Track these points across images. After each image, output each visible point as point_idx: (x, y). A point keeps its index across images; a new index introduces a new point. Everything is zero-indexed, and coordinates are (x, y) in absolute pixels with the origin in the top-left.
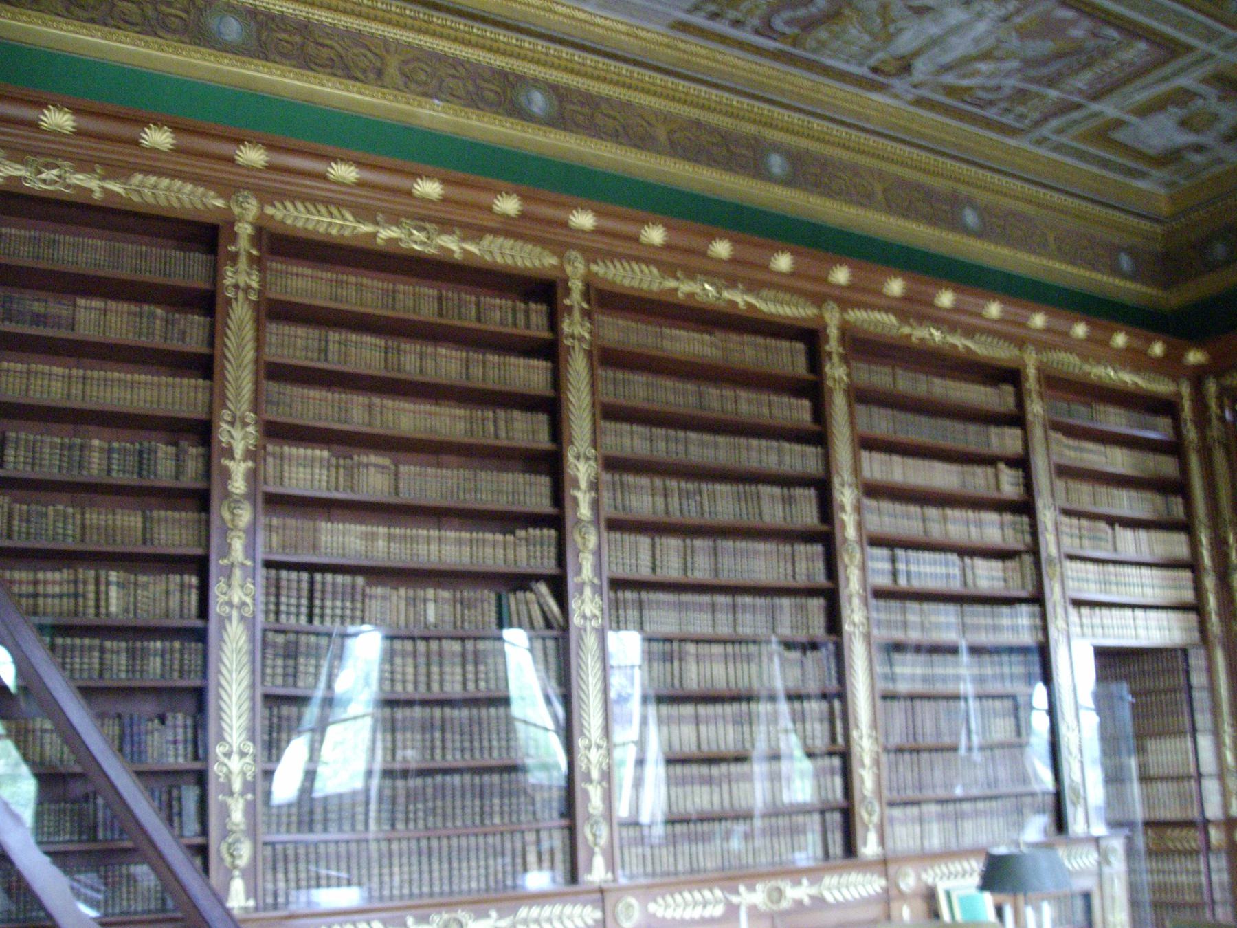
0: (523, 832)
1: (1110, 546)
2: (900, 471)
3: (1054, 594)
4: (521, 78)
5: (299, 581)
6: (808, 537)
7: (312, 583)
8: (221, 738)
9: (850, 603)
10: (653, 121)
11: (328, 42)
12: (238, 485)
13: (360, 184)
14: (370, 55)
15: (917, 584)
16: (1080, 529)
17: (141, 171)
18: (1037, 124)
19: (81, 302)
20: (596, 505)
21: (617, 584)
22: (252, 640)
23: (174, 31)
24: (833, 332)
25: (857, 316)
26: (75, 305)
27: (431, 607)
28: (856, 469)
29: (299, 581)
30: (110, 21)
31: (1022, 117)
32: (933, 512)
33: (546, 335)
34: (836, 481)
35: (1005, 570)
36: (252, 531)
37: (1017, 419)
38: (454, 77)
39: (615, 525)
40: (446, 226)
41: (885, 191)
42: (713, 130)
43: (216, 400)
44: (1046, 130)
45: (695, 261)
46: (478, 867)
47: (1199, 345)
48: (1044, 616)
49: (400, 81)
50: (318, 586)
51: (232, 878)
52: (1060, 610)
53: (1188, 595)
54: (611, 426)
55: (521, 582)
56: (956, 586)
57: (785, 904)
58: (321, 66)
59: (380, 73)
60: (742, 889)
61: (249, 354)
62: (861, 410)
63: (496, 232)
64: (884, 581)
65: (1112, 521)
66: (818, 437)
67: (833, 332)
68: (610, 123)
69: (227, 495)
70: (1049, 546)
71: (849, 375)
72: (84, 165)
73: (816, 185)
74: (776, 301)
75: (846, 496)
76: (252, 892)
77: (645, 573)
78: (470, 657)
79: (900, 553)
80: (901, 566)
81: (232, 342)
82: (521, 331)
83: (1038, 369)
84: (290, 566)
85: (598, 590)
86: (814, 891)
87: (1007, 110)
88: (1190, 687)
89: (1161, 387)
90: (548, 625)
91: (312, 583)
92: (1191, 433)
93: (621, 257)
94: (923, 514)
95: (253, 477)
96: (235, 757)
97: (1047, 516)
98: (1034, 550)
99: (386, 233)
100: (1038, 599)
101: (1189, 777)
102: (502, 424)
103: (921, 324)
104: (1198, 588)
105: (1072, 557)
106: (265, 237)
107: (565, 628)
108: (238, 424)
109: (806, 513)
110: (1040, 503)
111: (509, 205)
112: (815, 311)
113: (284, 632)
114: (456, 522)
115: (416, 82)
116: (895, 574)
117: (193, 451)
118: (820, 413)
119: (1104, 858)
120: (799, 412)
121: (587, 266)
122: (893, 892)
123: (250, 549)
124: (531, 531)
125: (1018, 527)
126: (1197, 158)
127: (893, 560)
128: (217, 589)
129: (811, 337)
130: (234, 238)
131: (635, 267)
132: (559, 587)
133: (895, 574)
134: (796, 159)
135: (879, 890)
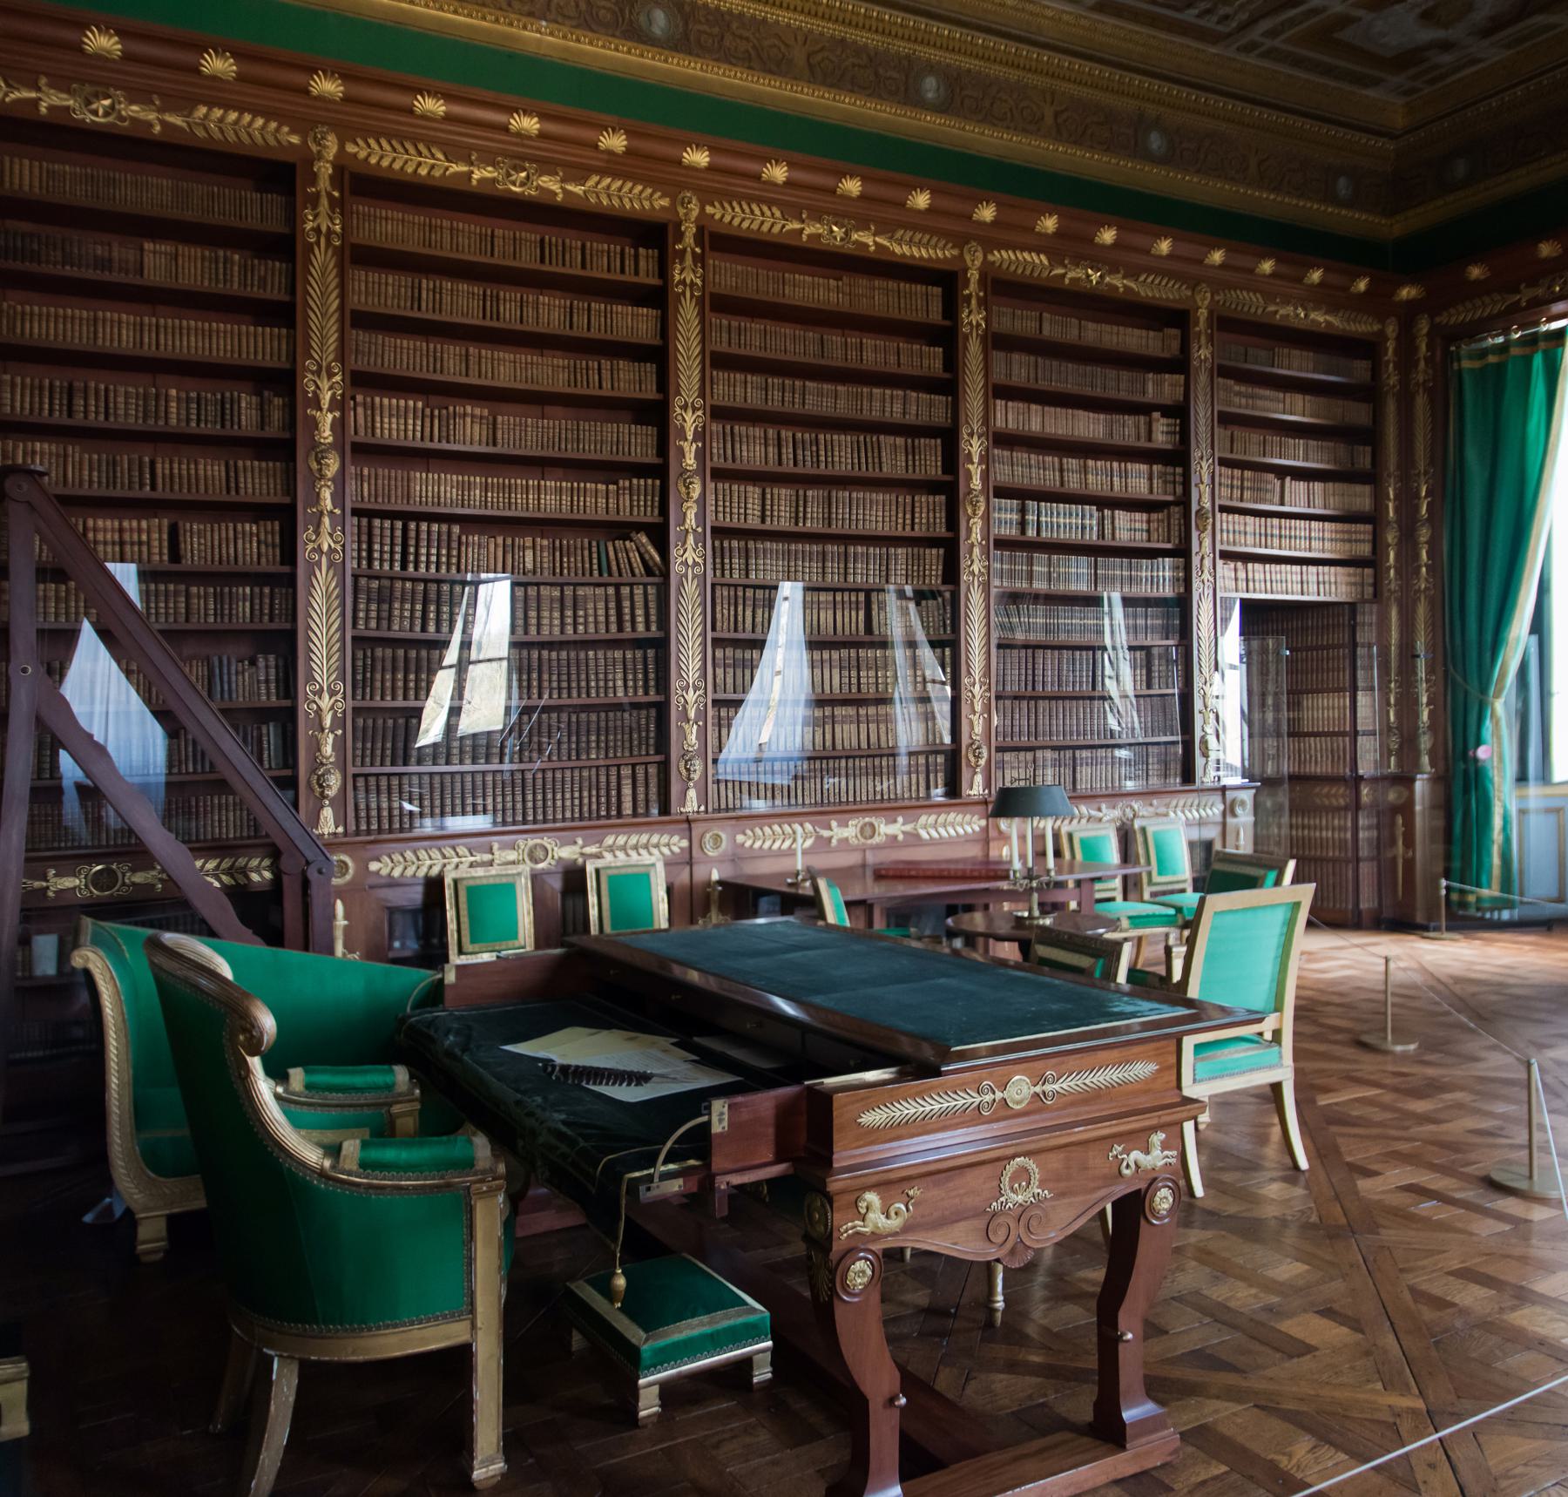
1: (1277, 499)
2: (1037, 420)
3: (1202, 546)
5: (392, 529)
6: (931, 487)
7: (405, 530)
8: (310, 678)
9: (971, 553)
12: (326, 434)
13: (448, 118)
16: (1242, 480)
17: (205, 104)
18: (1245, 27)
19: (148, 246)
20: (701, 455)
21: (719, 532)
22: (342, 584)
25: (1000, 256)
26: (142, 249)
27: (529, 554)
28: (986, 420)
29: (392, 529)
31: (1226, 17)
32: (1073, 463)
33: (654, 281)
34: (964, 432)
35: (1149, 522)
36: (340, 480)
37: (1180, 365)
39: (719, 475)
41: (1056, 115)
42: (859, 50)
43: (296, 349)
44: (1256, 33)
46: (573, 798)
47: (1412, 282)
48: (1188, 568)
50: (412, 534)
51: (322, 807)
52: (1208, 563)
53: (1365, 549)
54: (721, 375)
55: (621, 530)
56: (1092, 537)
57: (877, 840)
60: (834, 824)
62: (998, 356)
64: (1011, 532)
65: (1282, 472)
66: (948, 386)
69: (314, 445)
70: (1201, 496)
71: (986, 320)
74: (910, 242)
75: (974, 447)
76: (341, 819)
77: (753, 522)
78: (569, 603)
79: (1032, 505)
80: (1031, 517)
81: (315, 290)
82: (628, 277)
83: (1211, 313)
84: (384, 515)
85: (700, 539)
86: (908, 828)
87: (1208, 12)
88: (1354, 645)
89: (1363, 327)
90: (649, 571)
91: (405, 530)
92: (1392, 378)
94: (1061, 464)
95: (339, 426)
96: (326, 696)
97: (1203, 468)
98: (1184, 502)
99: (479, 174)
100: (1182, 552)
101: (1343, 734)
102: (606, 374)
103: (1077, 265)
104: (1377, 542)
105: (1223, 509)
106: (347, 176)
107: (666, 575)
108: (324, 373)
109: (930, 465)
110: (1195, 454)
112: (955, 252)
113: (377, 578)
116: (1023, 524)
117: (278, 401)
118: (952, 362)
119: (1230, 810)
120: (931, 360)
122: (992, 833)
123: (339, 498)
125: (1170, 478)
126: (1446, 58)
127: (1023, 511)
128: (305, 535)
129: (947, 280)
130: (313, 178)
131: (754, 207)
132: (660, 535)
133: (1023, 524)
134: (954, 81)
135: (977, 829)
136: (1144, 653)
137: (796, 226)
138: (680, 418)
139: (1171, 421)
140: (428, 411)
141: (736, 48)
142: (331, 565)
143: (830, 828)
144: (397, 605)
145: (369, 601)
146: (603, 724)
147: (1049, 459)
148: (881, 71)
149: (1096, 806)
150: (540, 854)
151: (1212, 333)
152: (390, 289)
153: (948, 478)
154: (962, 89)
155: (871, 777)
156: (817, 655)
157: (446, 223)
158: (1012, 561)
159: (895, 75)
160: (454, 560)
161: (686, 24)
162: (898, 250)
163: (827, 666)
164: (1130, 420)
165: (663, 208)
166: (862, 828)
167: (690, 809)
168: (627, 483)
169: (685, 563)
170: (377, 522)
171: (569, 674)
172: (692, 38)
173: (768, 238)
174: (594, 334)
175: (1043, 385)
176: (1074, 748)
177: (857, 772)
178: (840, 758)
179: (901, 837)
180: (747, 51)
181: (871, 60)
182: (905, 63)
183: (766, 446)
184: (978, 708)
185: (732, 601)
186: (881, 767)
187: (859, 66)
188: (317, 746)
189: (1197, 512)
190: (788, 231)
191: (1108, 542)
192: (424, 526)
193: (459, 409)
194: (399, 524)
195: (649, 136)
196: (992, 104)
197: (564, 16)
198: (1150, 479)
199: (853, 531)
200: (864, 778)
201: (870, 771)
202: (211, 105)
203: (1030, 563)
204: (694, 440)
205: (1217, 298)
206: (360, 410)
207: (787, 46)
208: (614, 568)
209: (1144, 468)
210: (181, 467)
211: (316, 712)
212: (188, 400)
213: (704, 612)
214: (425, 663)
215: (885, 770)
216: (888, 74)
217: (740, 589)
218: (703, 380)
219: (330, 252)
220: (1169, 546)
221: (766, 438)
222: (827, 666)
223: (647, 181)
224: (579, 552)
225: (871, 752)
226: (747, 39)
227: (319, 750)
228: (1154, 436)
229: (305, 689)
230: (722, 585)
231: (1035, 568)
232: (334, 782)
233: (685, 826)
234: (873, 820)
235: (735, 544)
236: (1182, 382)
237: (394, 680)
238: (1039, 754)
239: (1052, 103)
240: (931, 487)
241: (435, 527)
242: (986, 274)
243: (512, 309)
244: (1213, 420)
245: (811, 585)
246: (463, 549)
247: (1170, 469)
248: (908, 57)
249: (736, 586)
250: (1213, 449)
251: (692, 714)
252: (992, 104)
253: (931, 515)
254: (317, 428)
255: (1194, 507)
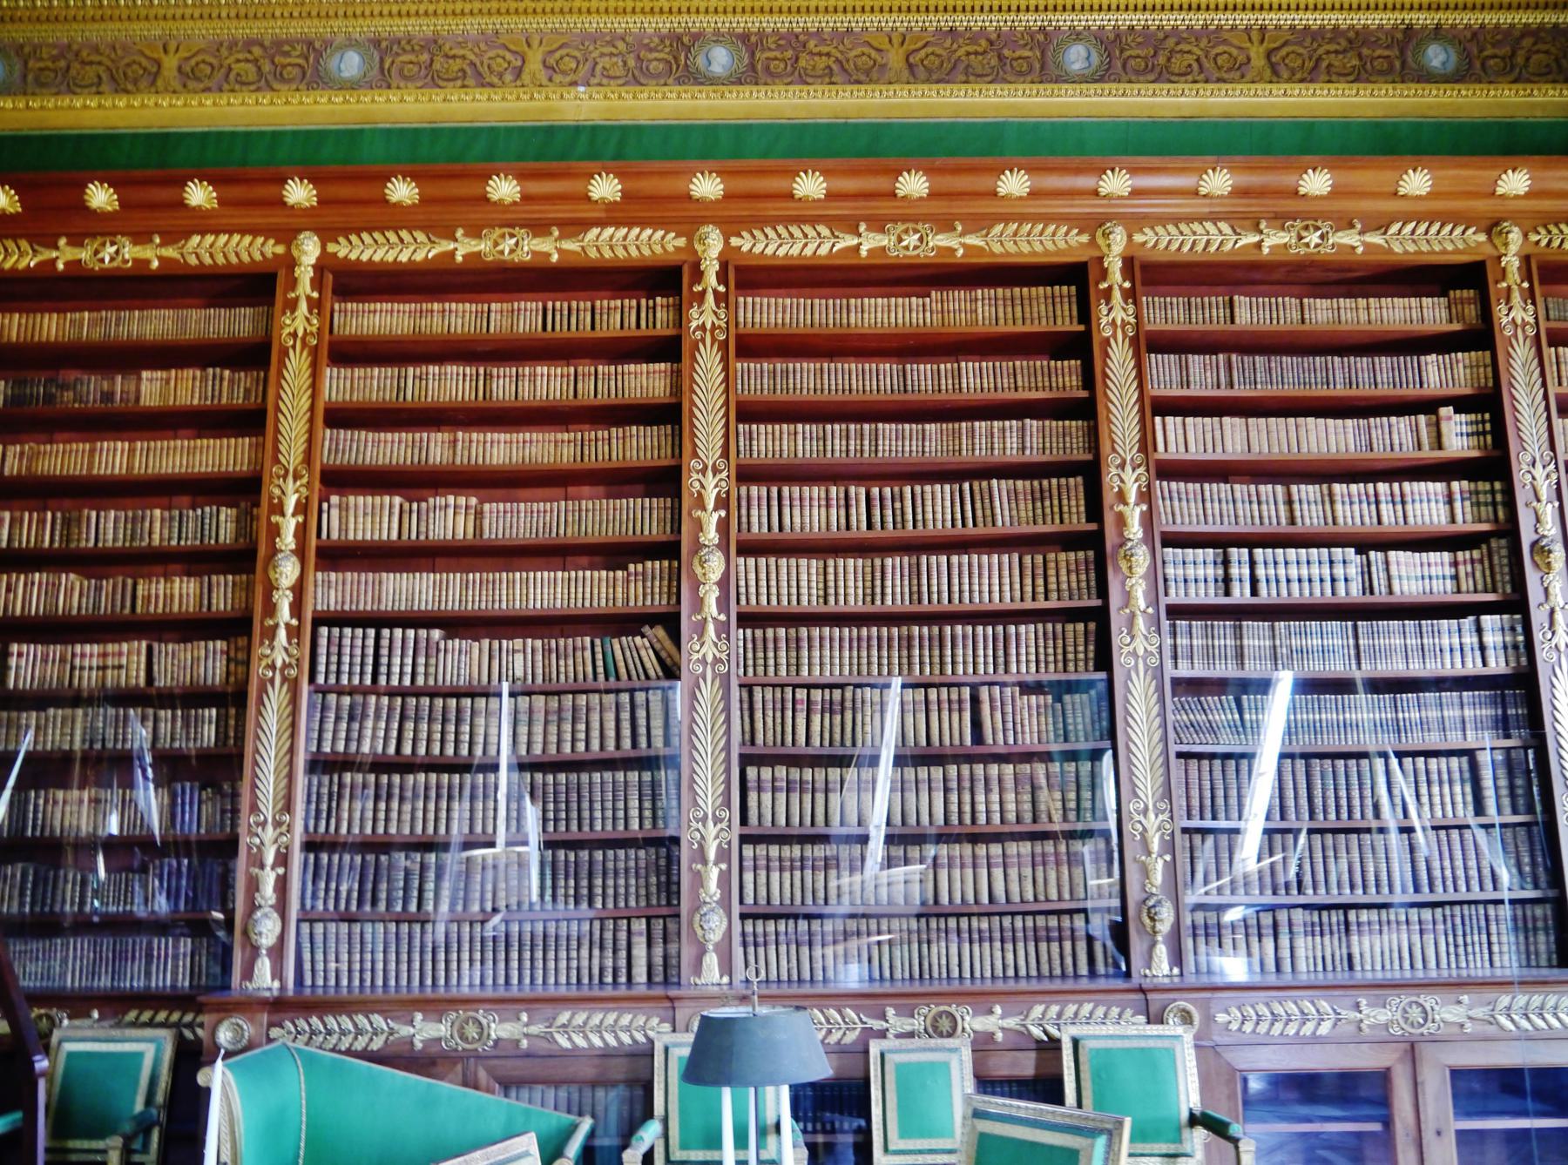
0: (629, 919)
4: (697, 37)
5: (364, 638)
6: (1069, 541)
7: (378, 638)
8: (254, 809)
10: (886, 46)
11: (461, 52)
12: (288, 540)
14: (509, 56)
15: (1266, 595)
19: (145, 374)
20: (723, 526)
23: (289, 81)
24: (1115, 265)
26: (140, 379)
27: (519, 658)
29: (364, 637)
30: (226, 87)
32: (1307, 492)
35: (1455, 564)
38: (612, 55)
39: (750, 548)
40: (539, 228)
41: (1269, 54)
42: (973, 37)
45: (883, 208)
49: (542, 76)
50: (385, 643)
56: (1353, 592)
58: (448, 80)
59: (518, 73)
61: (305, 403)
63: (602, 223)
67: (1115, 265)
68: (822, 62)
72: (141, 238)
73: (1147, 70)
77: (810, 602)
86: (1012, 1022)
91: (378, 638)
93: (773, 222)
96: (270, 828)
98: (1509, 530)
100: (1516, 604)
111: (605, 188)
114: (584, 560)
115: (564, 73)
121: (727, 242)
124: (649, 564)
136: (1465, 760)
137: (851, 241)
138: (697, 484)
139: (1473, 417)
140: (406, 506)
141: (814, 68)
142: (284, 679)
143: (884, 1017)
144: (369, 724)
145: (338, 719)
146: (610, 865)
147: (1266, 489)
148: (1006, 52)
149: (1453, 997)
150: (472, 1031)
151: (1531, 288)
152: (375, 383)
153: (1093, 527)
154: (1122, 51)
155: (998, 944)
156: (910, 773)
157: (436, 306)
158: (1209, 634)
159: (1027, 53)
160: (432, 670)
161: (753, 54)
162: (997, 249)
163: (924, 787)
164: (1401, 424)
165: (677, 249)
166: (935, 1020)
167: (709, 980)
168: (640, 567)
169: (704, 661)
170: (348, 631)
171: (567, 802)
172: (759, 67)
173: (762, 262)
174: (602, 398)
175: (1241, 391)
176: (1346, 907)
177: (976, 936)
178: (947, 916)
179: (999, 1036)
180: (829, 67)
181: (992, 43)
182: (1041, 37)
183: (828, 506)
184: (1155, 845)
185: (779, 706)
186: (1014, 930)
187: (976, 53)
188: (254, 885)
189: (1534, 544)
190: (840, 251)
191: (1380, 596)
192: (398, 632)
193: (440, 501)
194: (371, 632)
195: (652, 173)
196: (1169, 59)
197: (609, 77)
198: (1450, 501)
199: (956, 606)
200: (986, 945)
201: (997, 935)
202: (203, 233)
203: (1239, 635)
204: (716, 509)
205: (1534, 238)
206: (335, 513)
207: (879, 50)
208: (623, 671)
209: (1439, 487)
210: (159, 587)
211: (258, 848)
212: (171, 519)
213: (728, 721)
214: (397, 791)
215: (1020, 935)
216: (1018, 53)
217: (789, 690)
218: (726, 436)
219: (305, 353)
220: (1491, 597)
221: (828, 499)
222: (924, 787)
223: (655, 223)
224: (579, 654)
225: (994, 909)
226: (828, 55)
227: (258, 890)
228: (1445, 440)
229: (246, 819)
230: (763, 686)
231: (1245, 642)
232: (267, 929)
233: (669, 1004)
234: (953, 1009)
235: (782, 632)
236: (1488, 361)
237: (388, 810)
238: (1352, 915)
239: (1262, 41)
240: (1069, 541)
241: (411, 633)
242: (1132, 258)
243: (506, 385)
244: (1547, 408)
245: (910, 680)
246: (442, 655)
247: (1483, 486)
248: (1042, 29)
249: (782, 686)
250: (1552, 447)
251: (712, 854)
252: (1169, 59)
253: (1073, 577)
254: (279, 535)
255: (1527, 537)
